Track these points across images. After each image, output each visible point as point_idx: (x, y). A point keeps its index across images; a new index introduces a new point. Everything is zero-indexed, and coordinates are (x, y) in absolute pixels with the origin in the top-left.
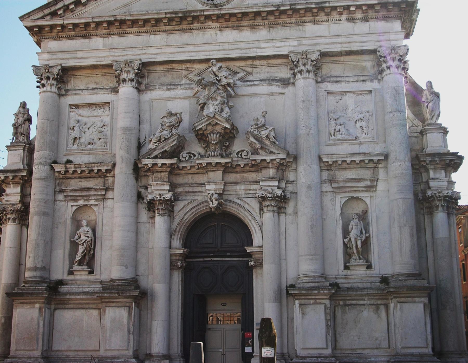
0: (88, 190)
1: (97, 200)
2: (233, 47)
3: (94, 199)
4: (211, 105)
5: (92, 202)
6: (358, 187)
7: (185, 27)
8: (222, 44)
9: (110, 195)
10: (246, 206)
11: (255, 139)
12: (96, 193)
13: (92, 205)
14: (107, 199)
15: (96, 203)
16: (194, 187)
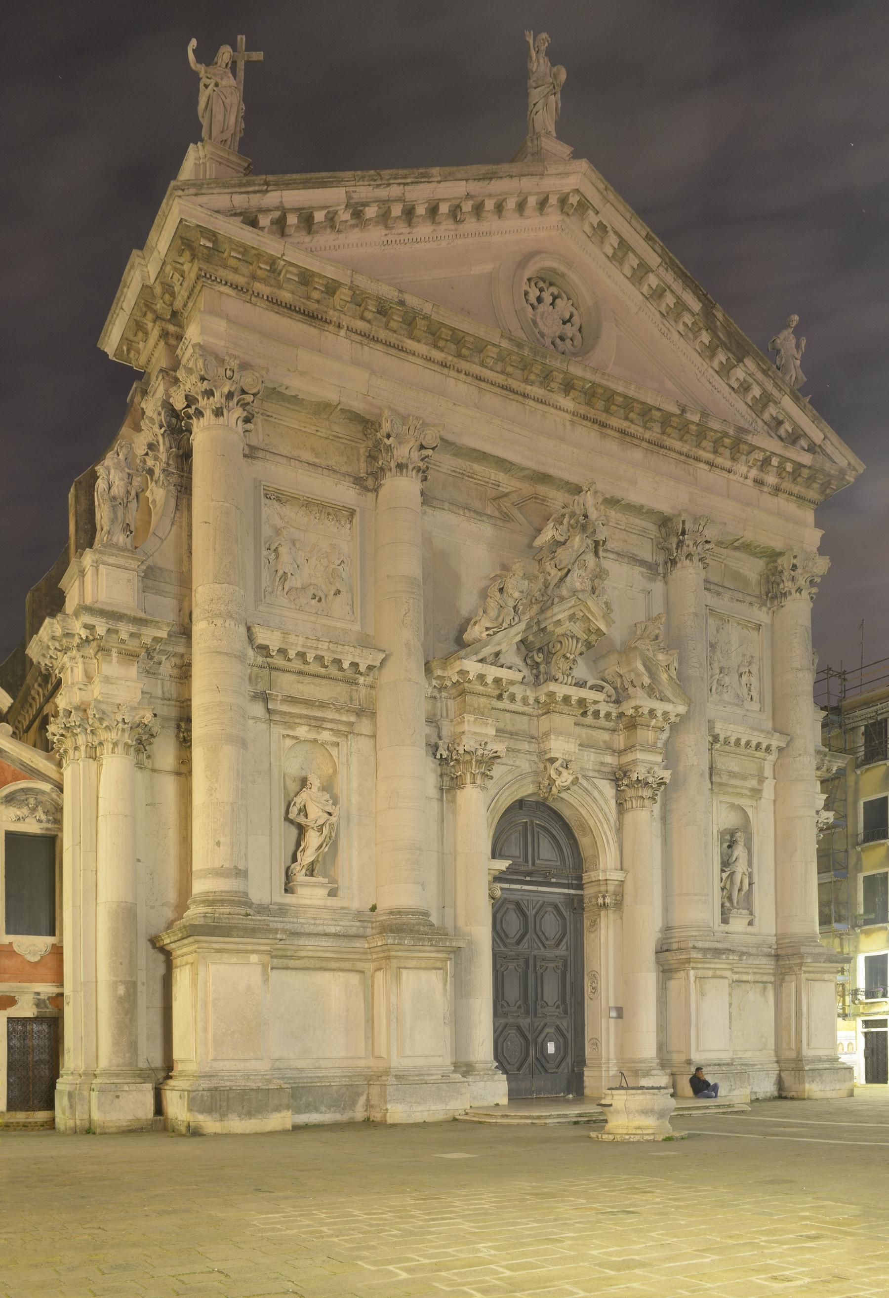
0: (323, 705)
1: (336, 732)
3: (332, 730)
4: (575, 575)
5: (326, 736)
6: (742, 788)
7: (515, 385)
9: (364, 726)
10: (596, 794)
11: (645, 665)
12: (337, 716)
13: (326, 743)
14: (358, 735)
15: (335, 739)
16: (517, 740)
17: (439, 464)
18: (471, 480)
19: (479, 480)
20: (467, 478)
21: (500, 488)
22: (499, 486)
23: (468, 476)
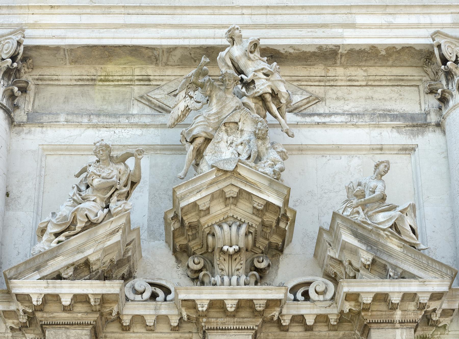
2: (279, 19)
8: (249, 11)
17: (55, 77)
18: (108, 83)
19: (118, 81)
20: (101, 83)
21: (151, 83)
22: (149, 80)
23: (101, 80)
